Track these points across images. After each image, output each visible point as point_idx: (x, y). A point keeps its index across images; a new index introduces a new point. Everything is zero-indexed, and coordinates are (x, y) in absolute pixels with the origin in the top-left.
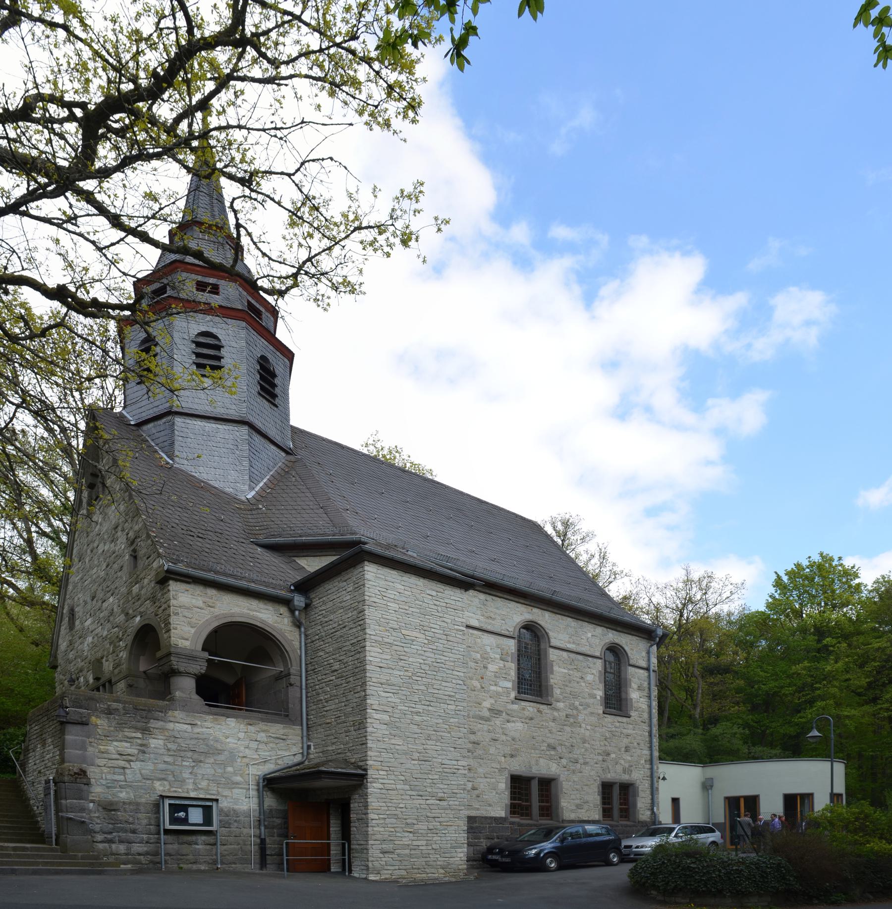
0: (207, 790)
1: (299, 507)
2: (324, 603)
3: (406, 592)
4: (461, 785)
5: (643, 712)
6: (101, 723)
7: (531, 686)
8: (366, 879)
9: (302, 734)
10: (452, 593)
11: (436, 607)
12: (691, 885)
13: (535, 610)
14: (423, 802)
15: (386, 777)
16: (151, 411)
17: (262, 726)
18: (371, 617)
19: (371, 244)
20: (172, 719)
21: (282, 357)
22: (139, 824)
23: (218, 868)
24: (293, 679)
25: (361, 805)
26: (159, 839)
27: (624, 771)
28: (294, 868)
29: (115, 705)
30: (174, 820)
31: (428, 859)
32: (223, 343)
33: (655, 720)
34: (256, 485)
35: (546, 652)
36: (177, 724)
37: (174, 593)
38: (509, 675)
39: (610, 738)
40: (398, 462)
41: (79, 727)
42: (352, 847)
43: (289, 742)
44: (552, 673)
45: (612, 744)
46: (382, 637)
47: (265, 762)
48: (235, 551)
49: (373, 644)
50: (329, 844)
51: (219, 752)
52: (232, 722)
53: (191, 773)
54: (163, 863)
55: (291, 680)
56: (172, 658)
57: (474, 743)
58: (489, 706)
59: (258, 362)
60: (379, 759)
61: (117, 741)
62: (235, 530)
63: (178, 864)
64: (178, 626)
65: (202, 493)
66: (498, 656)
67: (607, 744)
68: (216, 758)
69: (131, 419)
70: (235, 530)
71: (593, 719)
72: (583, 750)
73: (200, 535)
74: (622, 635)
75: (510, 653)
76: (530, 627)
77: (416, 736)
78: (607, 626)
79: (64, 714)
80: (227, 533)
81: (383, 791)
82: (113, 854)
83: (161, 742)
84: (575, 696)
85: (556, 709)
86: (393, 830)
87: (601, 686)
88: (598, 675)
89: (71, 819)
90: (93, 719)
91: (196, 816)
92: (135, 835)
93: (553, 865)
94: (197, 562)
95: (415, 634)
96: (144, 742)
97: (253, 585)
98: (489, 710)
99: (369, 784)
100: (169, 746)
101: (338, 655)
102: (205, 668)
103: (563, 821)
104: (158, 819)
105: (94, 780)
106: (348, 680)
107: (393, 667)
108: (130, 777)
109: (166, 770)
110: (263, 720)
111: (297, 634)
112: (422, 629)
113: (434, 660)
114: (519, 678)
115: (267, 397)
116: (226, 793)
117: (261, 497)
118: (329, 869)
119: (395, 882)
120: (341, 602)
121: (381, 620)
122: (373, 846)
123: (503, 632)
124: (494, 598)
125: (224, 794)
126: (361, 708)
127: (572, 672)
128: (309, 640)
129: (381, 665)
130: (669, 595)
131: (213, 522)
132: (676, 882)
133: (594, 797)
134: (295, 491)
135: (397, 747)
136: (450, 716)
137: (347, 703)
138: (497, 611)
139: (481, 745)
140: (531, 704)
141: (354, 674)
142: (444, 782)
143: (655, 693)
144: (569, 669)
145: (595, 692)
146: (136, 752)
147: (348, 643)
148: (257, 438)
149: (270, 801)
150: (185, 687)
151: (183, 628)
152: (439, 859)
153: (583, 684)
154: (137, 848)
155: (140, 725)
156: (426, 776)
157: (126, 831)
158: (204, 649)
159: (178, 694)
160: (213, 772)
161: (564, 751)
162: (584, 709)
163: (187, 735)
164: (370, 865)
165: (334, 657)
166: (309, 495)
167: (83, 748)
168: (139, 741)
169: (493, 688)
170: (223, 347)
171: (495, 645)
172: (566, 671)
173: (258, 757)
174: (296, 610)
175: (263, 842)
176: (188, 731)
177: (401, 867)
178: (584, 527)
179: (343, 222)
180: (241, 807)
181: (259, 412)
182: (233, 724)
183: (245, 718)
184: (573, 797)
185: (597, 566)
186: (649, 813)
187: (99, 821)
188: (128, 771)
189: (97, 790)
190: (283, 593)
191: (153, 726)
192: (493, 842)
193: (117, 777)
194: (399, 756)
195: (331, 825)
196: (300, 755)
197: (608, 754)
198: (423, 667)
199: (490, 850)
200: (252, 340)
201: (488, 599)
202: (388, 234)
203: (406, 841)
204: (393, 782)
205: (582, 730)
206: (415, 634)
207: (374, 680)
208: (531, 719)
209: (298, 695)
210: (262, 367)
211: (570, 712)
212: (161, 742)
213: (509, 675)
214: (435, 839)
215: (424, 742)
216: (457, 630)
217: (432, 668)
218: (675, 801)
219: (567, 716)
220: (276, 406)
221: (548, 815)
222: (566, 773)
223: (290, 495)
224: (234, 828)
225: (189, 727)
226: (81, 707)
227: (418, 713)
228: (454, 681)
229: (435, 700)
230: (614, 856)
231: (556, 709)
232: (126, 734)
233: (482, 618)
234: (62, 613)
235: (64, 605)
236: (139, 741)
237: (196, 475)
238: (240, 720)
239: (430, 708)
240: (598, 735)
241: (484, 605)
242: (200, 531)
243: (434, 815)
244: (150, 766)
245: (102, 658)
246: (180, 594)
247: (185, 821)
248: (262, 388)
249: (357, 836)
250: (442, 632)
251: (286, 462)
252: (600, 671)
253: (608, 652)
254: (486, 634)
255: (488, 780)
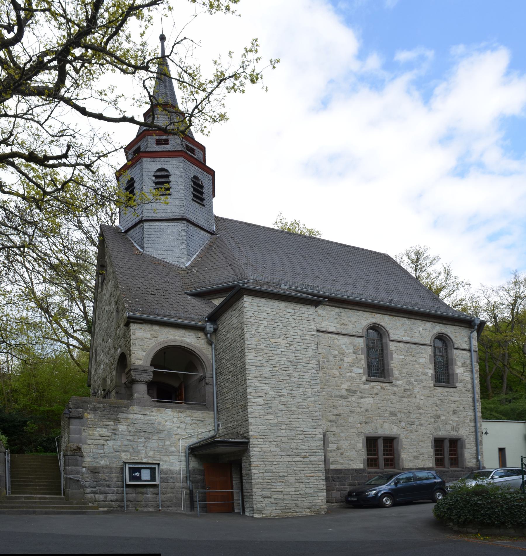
0: (153, 458)
1: (216, 267)
2: (224, 327)
3: (272, 313)
4: (319, 446)
5: (467, 383)
6: (90, 416)
7: (378, 370)
8: (252, 517)
9: (214, 417)
10: (305, 309)
11: (294, 321)
12: (478, 518)
13: (377, 315)
14: (291, 460)
15: (262, 443)
16: (132, 223)
17: (188, 412)
18: (248, 332)
19: (233, 88)
20: (132, 412)
21: (207, 174)
22: (112, 481)
23: (159, 510)
24: (208, 380)
25: (247, 463)
26: (123, 491)
27: (453, 429)
28: (207, 509)
29: (98, 405)
30: (132, 478)
31: (297, 502)
32: (171, 173)
33: (477, 389)
34: (192, 257)
35: (387, 344)
36: (135, 415)
37: (133, 331)
38: (360, 364)
39: (440, 405)
40: (298, 231)
41: (77, 421)
42: (245, 494)
43: (206, 422)
44: (392, 360)
45: (442, 409)
46: (256, 345)
47: (190, 437)
48: (173, 300)
49: (250, 351)
50: (232, 492)
51: (161, 432)
52: (169, 411)
53: (143, 446)
54: (125, 507)
55: (207, 380)
56: (132, 372)
57: (337, 415)
58: (346, 388)
59: (192, 180)
60: (258, 431)
61: (99, 428)
62: (176, 287)
63: (136, 507)
64: (136, 352)
65: (159, 267)
66: (351, 351)
67: (437, 409)
68: (159, 435)
69: (122, 229)
70: (176, 287)
71: (426, 391)
72: (418, 415)
73: (153, 293)
74: (447, 326)
75: (360, 348)
76: (375, 328)
77: (283, 412)
78: (435, 321)
79: (68, 412)
80: (170, 289)
81: (261, 453)
82: (96, 501)
83: (125, 427)
84: (411, 375)
85: (397, 386)
86: (269, 481)
87: (432, 366)
88: (429, 358)
89: (71, 478)
90: (86, 414)
91: (146, 475)
92: (109, 488)
93: (388, 503)
94: (147, 310)
95: (279, 341)
96: (115, 427)
97: (181, 320)
98: (347, 390)
99: (251, 449)
100: (130, 429)
101: (232, 361)
102: (152, 377)
103: (403, 469)
104: (123, 477)
105: (86, 453)
106: (238, 377)
107: (265, 365)
108: (106, 450)
109: (128, 445)
110: (188, 409)
111: (210, 349)
112: (285, 336)
113: (294, 358)
114: (368, 365)
115: (198, 201)
116: (166, 459)
117: (195, 264)
118: (233, 510)
119: (273, 519)
120: (233, 325)
121: (255, 333)
122: (256, 493)
123: (354, 334)
124: (346, 310)
125: (164, 460)
126: (244, 396)
127: (407, 358)
128: (218, 353)
129: (256, 364)
130: (501, 294)
131: (163, 284)
132: (466, 515)
133: (429, 450)
134: (215, 257)
135: (270, 421)
136: (308, 396)
137: (237, 393)
138: (349, 319)
139: (342, 416)
140: (379, 383)
141: (241, 373)
142: (306, 444)
143: (476, 367)
144: (405, 356)
145: (427, 371)
146: (110, 434)
147: (237, 352)
148: (192, 228)
149: (194, 464)
150: (140, 391)
151: (139, 352)
152: (305, 501)
153: (417, 366)
154: (111, 497)
155: (113, 416)
156: (292, 441)
157: (104, 486)
158: (151, 365)
159: (136, 395)
160: (157, 445)
161: (403, 416)
162: (418, 384)
163: (141, 421)
164: (255, 506)
165: (230, 362)
166: (223, 258)
167: (80, 433)
168: (112, 427)
169: (349, 374)
170: (170, 175)
171: (348, 343)
172: (403, 357)
173: (185, 434)
174: (208, 333)
175: (191, 492)
176: (142, 419)
177: (277, 508)
178: (431, 253)
179: (215, 79)
180: (175, 468)
181: (192, 211)
182: (170, 413)
183: (177, 408)
184: (411, 450)
185: (443, 280)
186: (474, 461)
187: (88, 480)
188: (105, 447)
189: (88, 460)
190: (200, 324)
191: (120, 417)
192: (354, 487)
193: (99, 451)
194: (272, 428)
195: (233, 479)
196: (213, 431)
197: (439, 417)
198: (286, 363)
199: (350, 494)
200: (187, 168)
201: (342, 311)
202: (241, 78)
203: (280, 489)
204: (268, 446)
205: (417, 400)
206: (279, 341)
207: (251, 375)
208: (377, 394)
209: (212, 391)
210: (194, 183)
211: (407, 387)
212: (125, 427)
213: (360, 364)
214: (301, 486)
215: (289, 416)
216: (310, 335)
217: (293, 363)
218: (502, 451)
219: (405, 390)
220: (204, 206)
221: (392, 465)
222: (405, 433)
223: (212, 260)
224: (170, 483)
225: (142, 416)
226: (78, 408)
227: (284, 396)
228: (309, 371)
229: (296, 386)
230: (439, 495)
231: (397, 386)
232: (105, 423)
233: (338, 326)
234: (93, 352)
235: (93, 347)
236: (112, 427)
237: (156, 257)
238: (174, 410)
239: (293, 392)
240: (430, 403)
241: (339, 316)
242: (153, 290)
243: (300, 469)
244: (119, 443)
245: (106, 377)
246: (137, 331)
247: (139, 478)
248: (195, 196)
249: (246, 486)
250: (299, 337)
251: (211, 240)
252: (430, 355)
253: (437, 340)
254: (341, 336)
255: (349, 442)
